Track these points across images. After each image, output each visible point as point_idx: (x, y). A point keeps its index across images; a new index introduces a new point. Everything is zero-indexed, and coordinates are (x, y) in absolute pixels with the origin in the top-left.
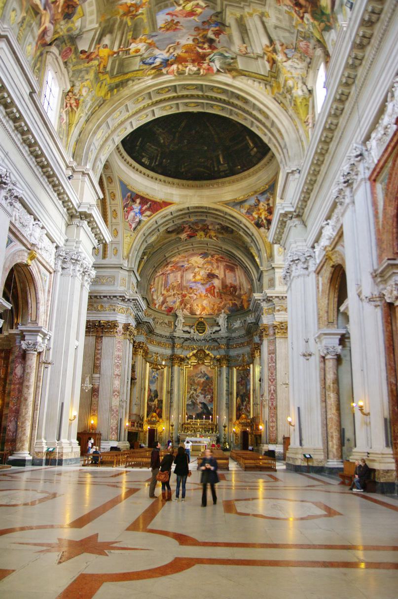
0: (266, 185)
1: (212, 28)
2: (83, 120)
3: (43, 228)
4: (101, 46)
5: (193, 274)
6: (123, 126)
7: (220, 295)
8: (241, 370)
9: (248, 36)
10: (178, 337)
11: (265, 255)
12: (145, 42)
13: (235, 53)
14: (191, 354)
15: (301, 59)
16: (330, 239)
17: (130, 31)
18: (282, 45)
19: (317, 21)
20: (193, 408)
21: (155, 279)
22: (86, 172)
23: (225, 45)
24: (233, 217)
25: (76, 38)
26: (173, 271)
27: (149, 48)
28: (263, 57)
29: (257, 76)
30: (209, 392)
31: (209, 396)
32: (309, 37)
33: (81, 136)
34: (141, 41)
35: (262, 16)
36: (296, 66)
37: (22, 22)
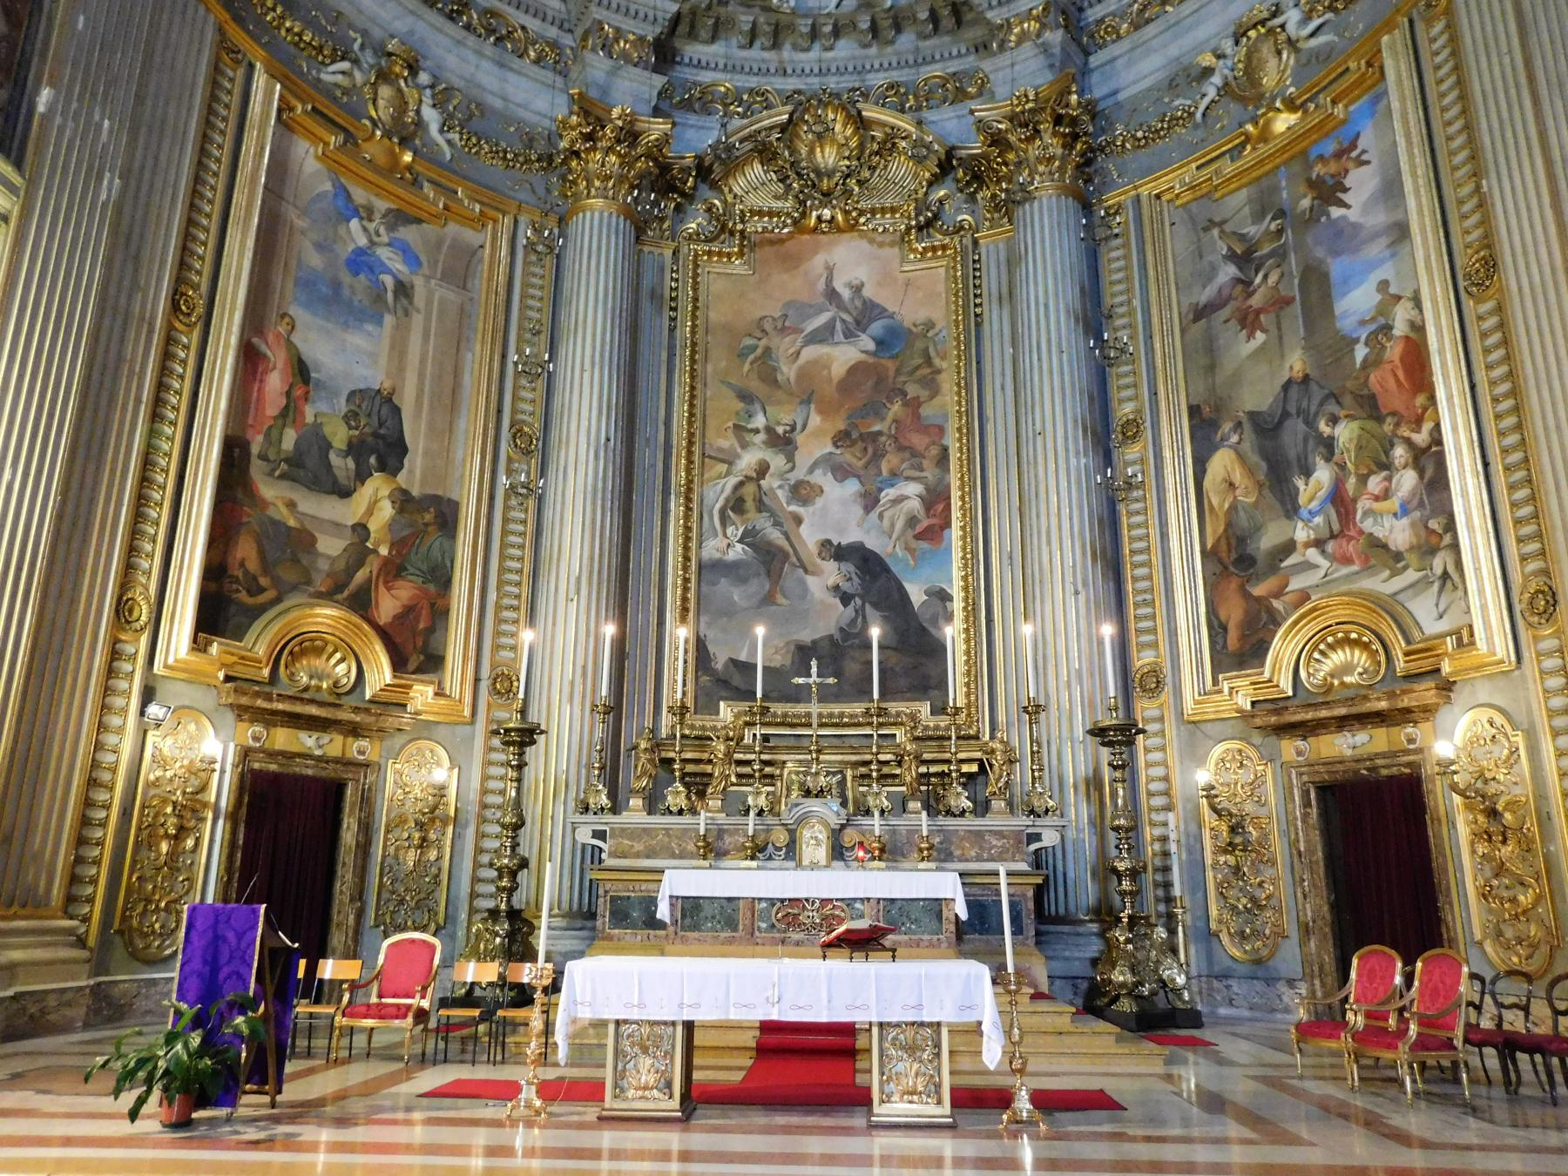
20: (768, 599)
30: (901, 448)
31: (913, 489)
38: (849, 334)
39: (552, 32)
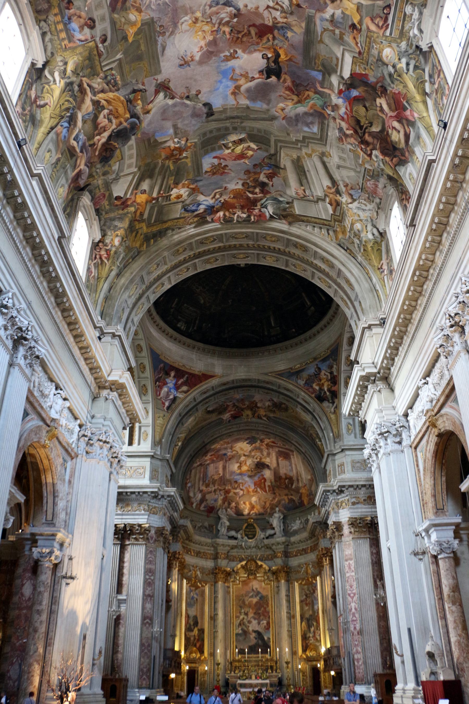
0: (328, 349)
1: (265, 172)
2: (113, 273)
3: (65, 399)
4: (139, 191)
5: (238, 465)
6: (160, 281)
7: (273, 489)
8: (304, 585)
9: (306, 178)
10: (223, 545)
11: (331, 435)
12: (188, 187)
13: (291, 197)
14: (239, 566)
15: (370, 200)
16: (431, 401)
17: (172, 175)
18: (346, 186)
19: (388, 157)
20: (245, 639)
21: (191, 471)
22: (117, 334)
23: (280, 188)
24: (288, 390)
25: (112, 182)
26: (213, 462)
27: (193, 194)
28: (324, 200)
29: (317, 220)
30: (264, 615)
31: (265, 622)
32: (378, 175)
33: (112, 290)
34: (183, 187)
35: (322, 156)
36: (364, 207)
37: (57, 163)
38: (256, 596)
39: (212, 552)
